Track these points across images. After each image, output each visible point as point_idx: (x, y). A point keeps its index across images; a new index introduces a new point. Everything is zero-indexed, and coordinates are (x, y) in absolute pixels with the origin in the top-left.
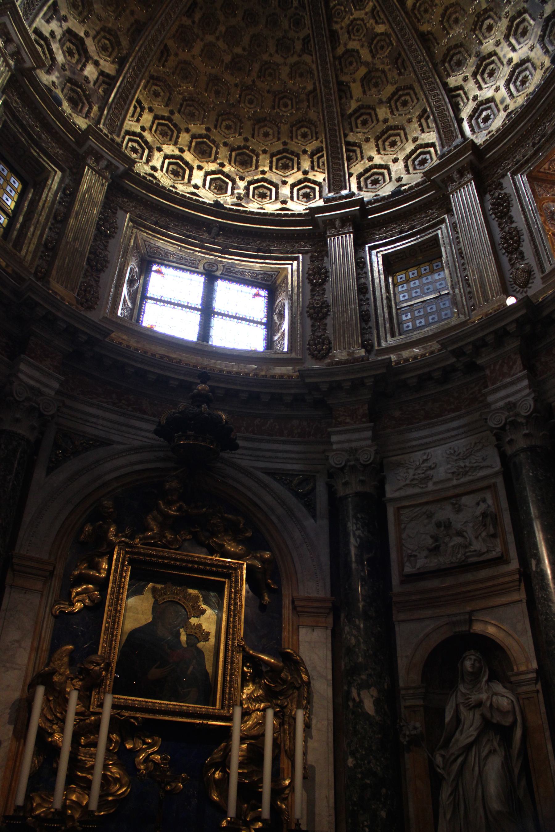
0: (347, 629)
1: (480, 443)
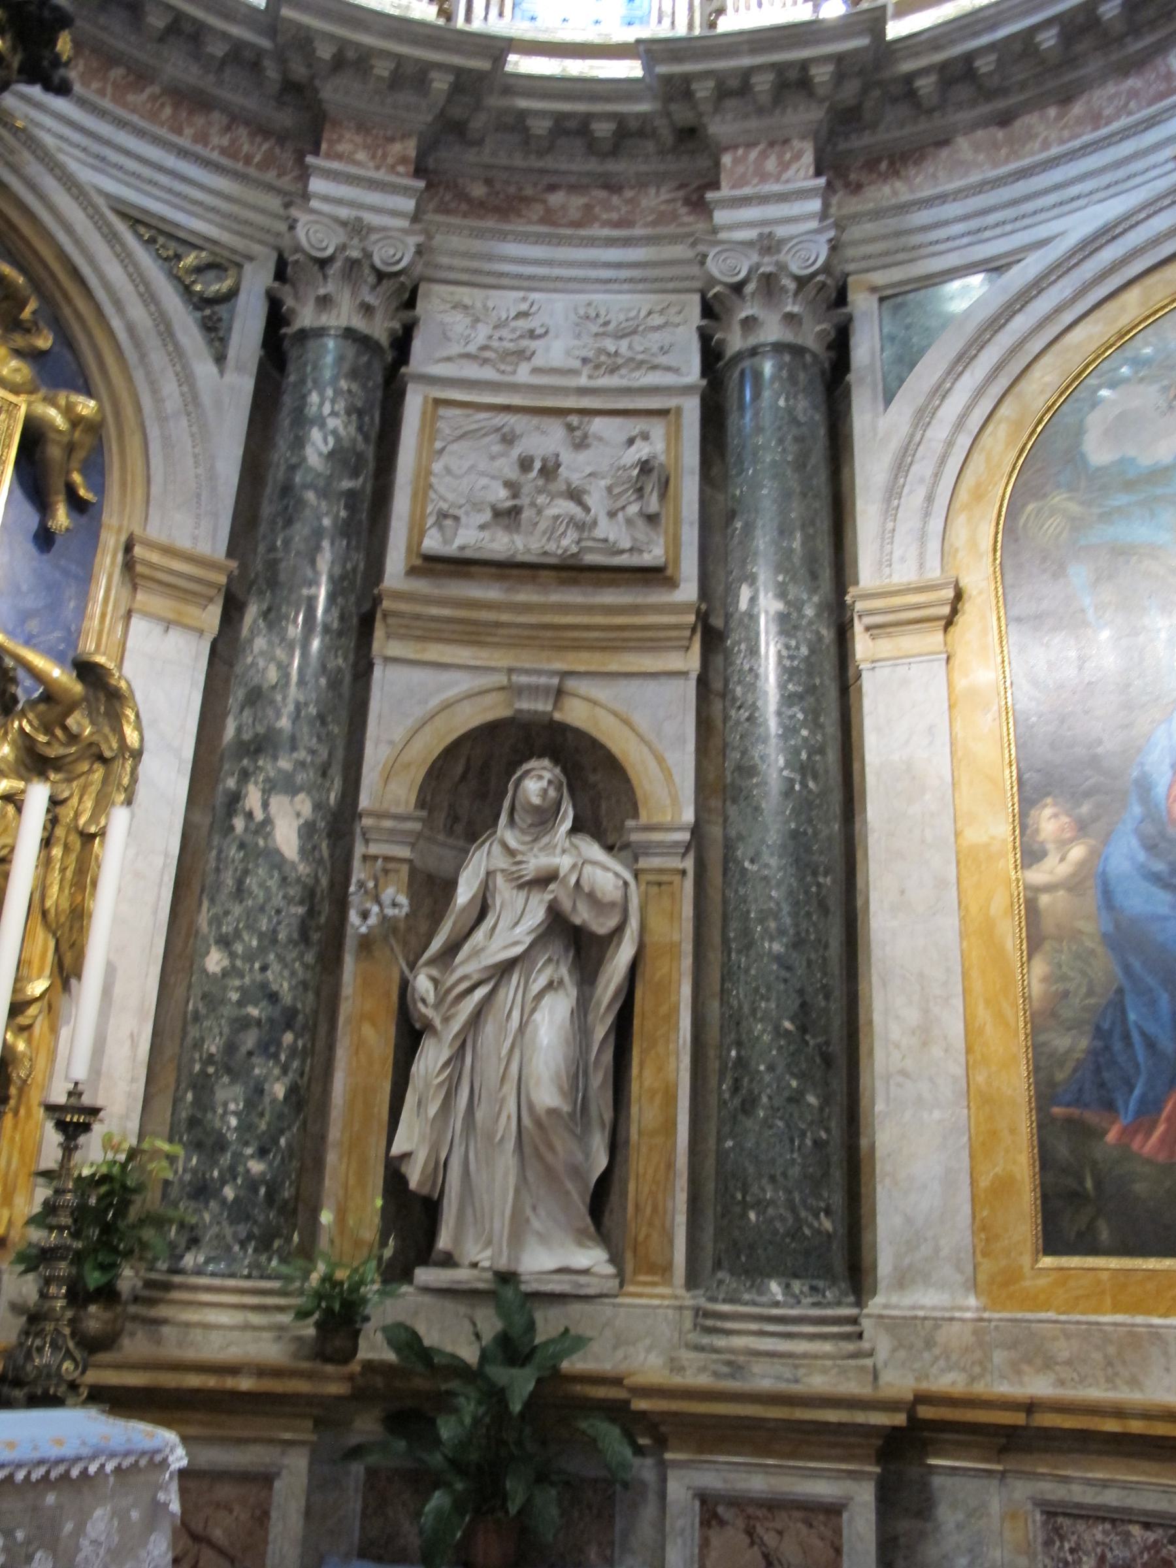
0: (260, 643)
1: (662, 312)
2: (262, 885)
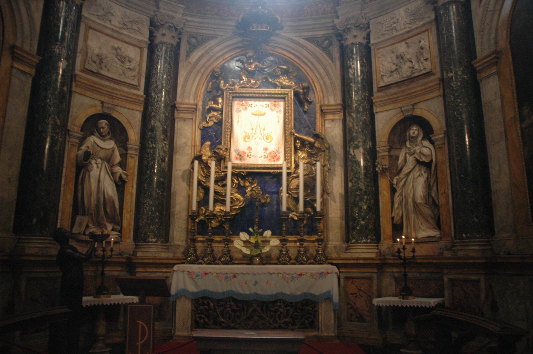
2: (356, 168)
